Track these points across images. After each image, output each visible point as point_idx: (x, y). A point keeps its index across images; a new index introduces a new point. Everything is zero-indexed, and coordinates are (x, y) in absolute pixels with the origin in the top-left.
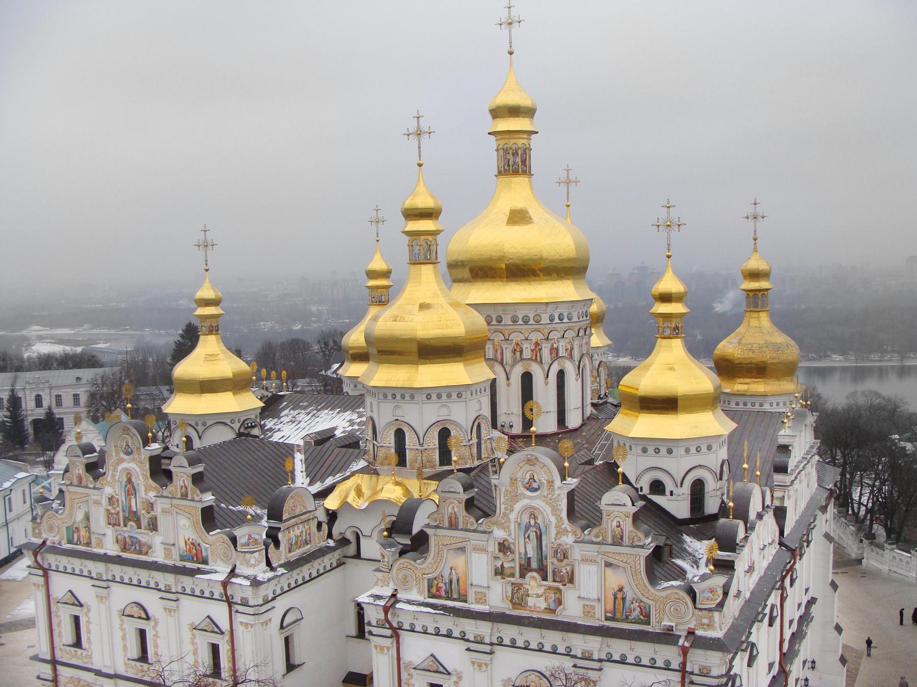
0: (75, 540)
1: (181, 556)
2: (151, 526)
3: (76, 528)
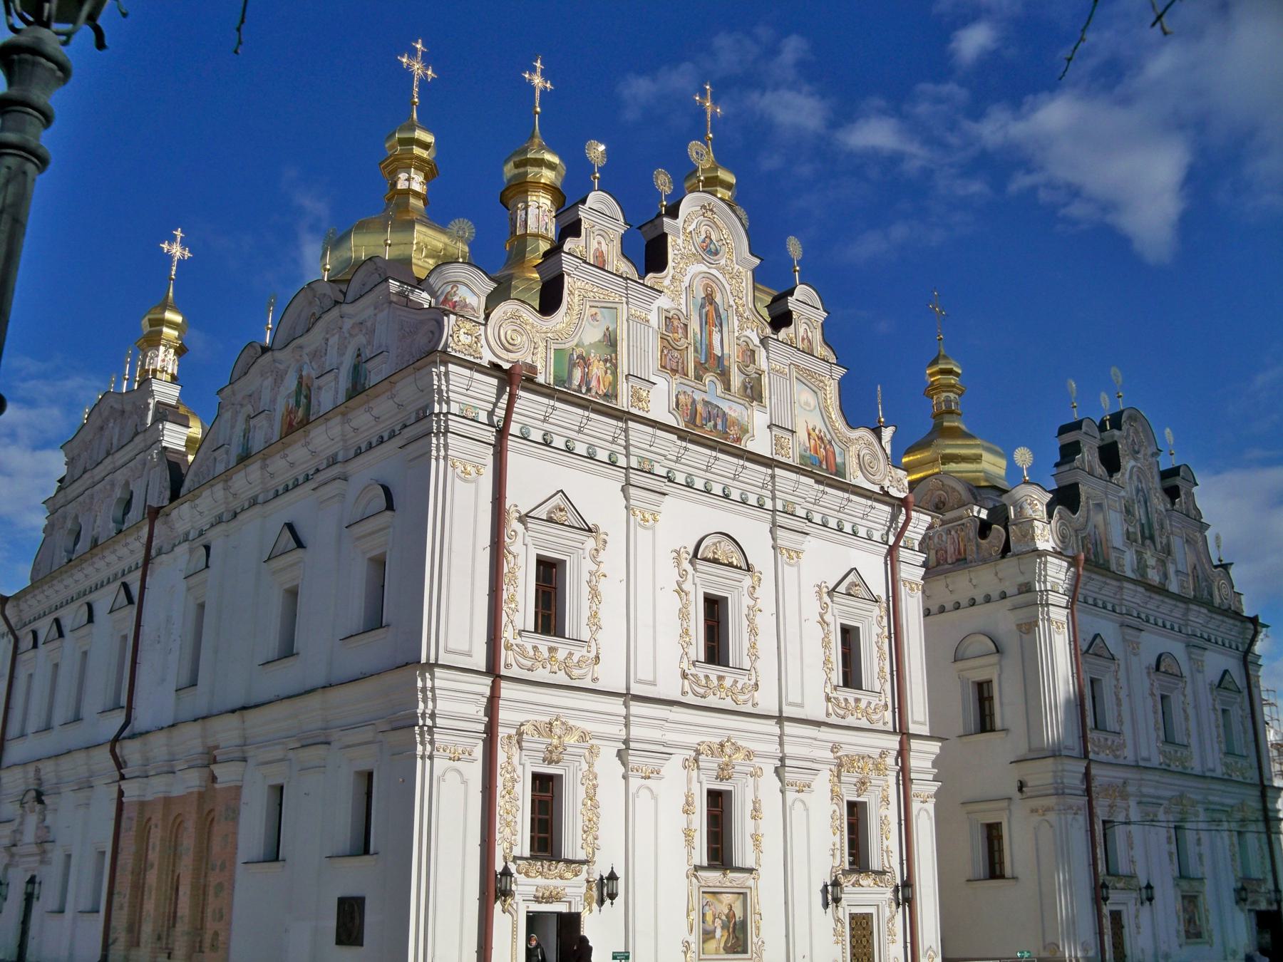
0: (576, 382)
1: (802, 457)
2: (749, 391)
3: (581, 357)
